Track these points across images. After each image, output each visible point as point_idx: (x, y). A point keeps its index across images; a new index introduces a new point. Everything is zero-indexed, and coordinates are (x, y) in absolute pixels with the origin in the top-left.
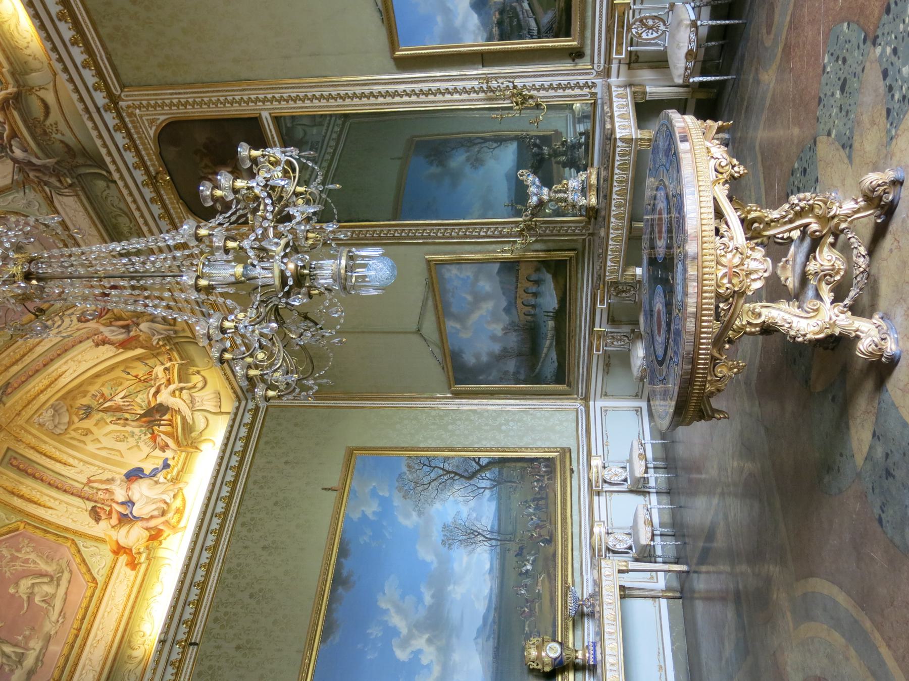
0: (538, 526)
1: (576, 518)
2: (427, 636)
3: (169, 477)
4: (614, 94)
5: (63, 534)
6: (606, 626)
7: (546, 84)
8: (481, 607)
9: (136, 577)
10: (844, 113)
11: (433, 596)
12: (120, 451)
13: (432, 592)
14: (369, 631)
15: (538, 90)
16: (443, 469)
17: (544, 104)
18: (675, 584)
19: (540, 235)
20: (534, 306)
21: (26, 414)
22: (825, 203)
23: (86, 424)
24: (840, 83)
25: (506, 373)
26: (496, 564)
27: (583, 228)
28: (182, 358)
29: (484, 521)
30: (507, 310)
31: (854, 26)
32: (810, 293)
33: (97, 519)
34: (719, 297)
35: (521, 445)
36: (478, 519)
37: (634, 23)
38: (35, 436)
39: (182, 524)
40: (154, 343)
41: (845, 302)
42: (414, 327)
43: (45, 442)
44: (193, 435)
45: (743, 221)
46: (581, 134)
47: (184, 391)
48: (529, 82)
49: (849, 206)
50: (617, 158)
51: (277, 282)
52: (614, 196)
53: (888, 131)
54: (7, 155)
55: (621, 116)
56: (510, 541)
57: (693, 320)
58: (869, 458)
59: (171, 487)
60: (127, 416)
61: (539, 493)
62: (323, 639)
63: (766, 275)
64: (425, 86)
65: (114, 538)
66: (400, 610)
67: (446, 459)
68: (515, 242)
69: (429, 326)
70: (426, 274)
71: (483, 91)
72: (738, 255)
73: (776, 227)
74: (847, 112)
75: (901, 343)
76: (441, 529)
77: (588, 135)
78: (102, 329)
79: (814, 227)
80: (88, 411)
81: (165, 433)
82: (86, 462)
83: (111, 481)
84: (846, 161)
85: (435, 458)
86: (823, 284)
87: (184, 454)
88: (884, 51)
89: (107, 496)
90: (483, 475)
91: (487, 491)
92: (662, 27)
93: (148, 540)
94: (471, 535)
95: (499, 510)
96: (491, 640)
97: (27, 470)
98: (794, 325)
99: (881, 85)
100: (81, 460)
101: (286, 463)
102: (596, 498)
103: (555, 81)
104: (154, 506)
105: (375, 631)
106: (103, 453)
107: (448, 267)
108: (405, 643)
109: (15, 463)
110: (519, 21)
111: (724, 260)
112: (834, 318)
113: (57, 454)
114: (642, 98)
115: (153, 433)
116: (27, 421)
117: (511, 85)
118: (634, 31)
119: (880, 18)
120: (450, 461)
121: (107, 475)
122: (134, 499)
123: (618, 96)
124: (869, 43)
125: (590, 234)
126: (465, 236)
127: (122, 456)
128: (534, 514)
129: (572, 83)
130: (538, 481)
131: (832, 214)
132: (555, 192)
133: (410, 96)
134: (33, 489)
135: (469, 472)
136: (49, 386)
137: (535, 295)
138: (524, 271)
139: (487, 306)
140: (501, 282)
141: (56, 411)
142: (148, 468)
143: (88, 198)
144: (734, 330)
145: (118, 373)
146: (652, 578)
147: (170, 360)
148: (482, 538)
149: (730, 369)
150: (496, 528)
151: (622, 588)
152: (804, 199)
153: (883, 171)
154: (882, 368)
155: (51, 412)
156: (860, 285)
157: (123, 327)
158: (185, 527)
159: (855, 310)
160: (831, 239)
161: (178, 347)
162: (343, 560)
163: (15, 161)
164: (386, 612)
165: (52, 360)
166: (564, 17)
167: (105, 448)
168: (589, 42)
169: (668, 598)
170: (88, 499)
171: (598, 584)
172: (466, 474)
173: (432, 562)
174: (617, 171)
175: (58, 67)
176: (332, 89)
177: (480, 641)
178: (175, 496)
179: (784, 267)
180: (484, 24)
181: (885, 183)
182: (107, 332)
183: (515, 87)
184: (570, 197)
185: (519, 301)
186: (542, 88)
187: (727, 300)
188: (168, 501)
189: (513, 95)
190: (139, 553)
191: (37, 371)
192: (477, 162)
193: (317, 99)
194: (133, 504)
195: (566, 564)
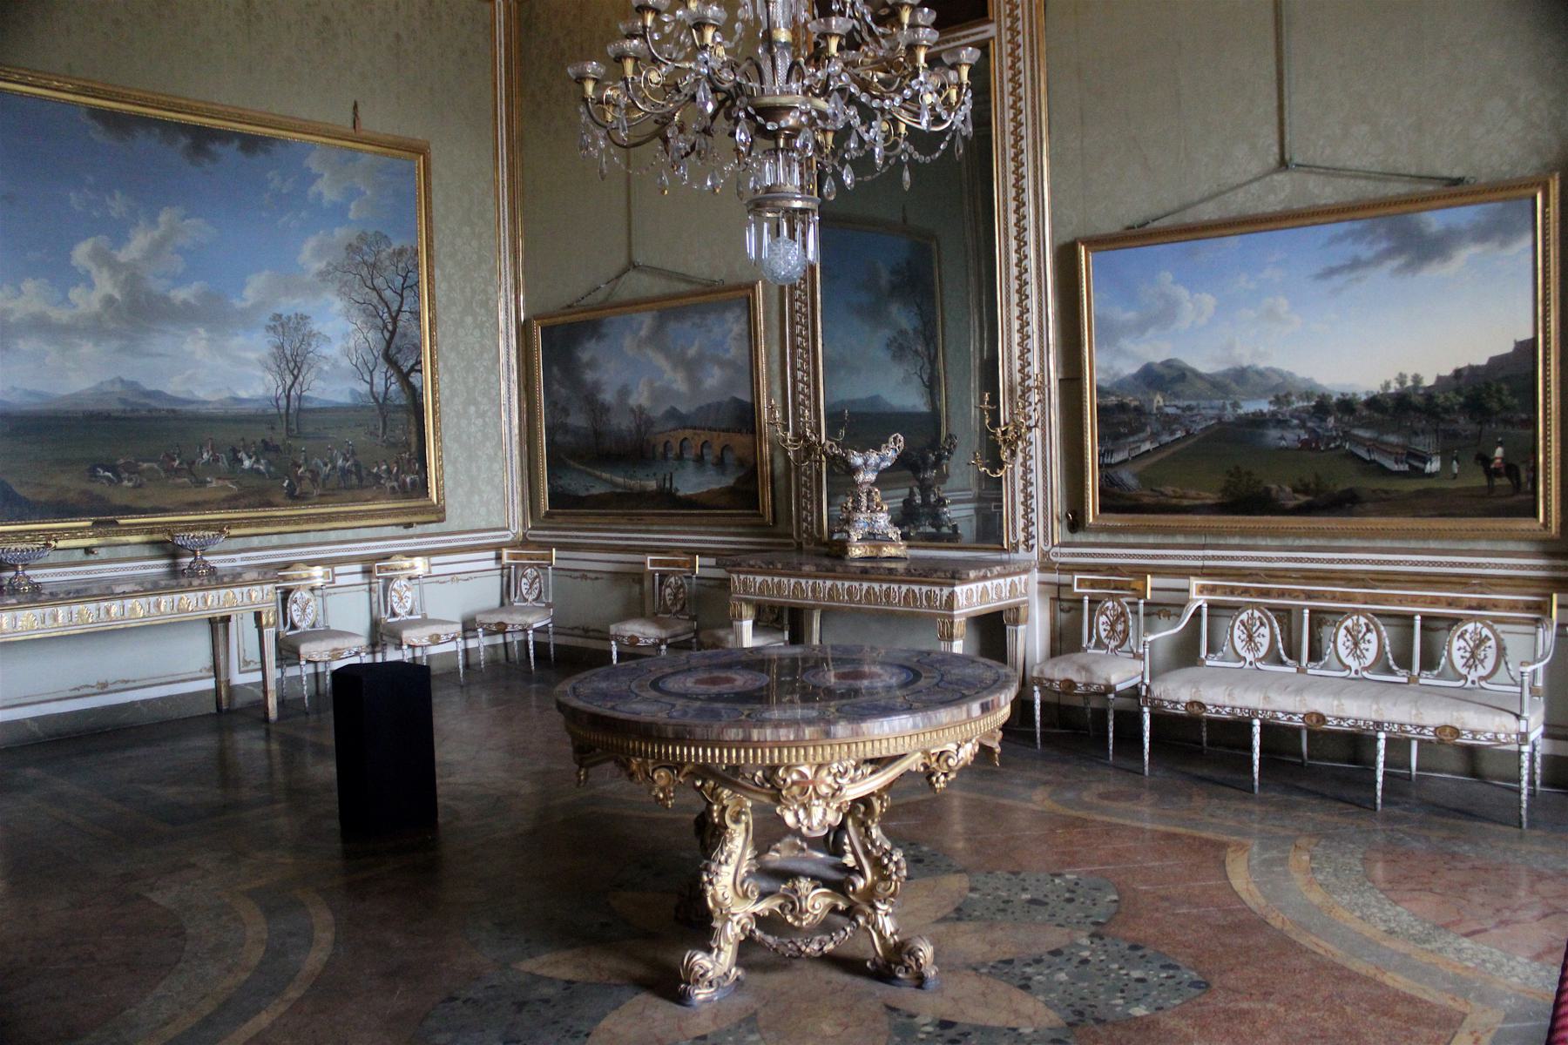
0: (315, 474)
1: (333, 536)
2: (118, 296)
4: (1016, 579)
6: (168, 598)
7: (1032, 477)
8: (174, 386)
10: (1002, 906)
11: (185, 303)
13: (193, 301)
14: (118, 194)
15: (1024, 464)
16: (399, 310)
17: (1001, 473)
18: (239, 701)
19: (797, 468)
20: (680, 457)
22: (892, 895)
24: (1041, 897)
25: (565, 411)
26: (250, 408)
27: (811, 534)
30: (673, 414)
31: (1113, 907)
32: (765, 885)
34: (774, 769)
35: (446, 440)
36: (320, 374)
37: (1120, 604)
41: (758, 933)
42: (639, 259)
45: (872, 794)
46: (955, 527)
48: (1036, 450)
49: (888, 925)
50: (925, 589)
51: (767, 100)
52: (865, 585)
53: (984, 964)
55: (985, 591)
56: (288, 429)
57: (740, 737)
58: (538, 979)
61: (370, 473)
62: (95, 113)
63: (804, 830)
64: (1032, 289)
66: (156, 249)
67: (417, 315)
68: (786, 428)
70: (730, 281)
71: (1023, 380)
72: (830, 791)
73: (858, 833)
74: (1004, 910)
75: (706, 1006)
76: (300, 310)
77: (952, 538)
79: (860, 884)
84: (939, 915)
85: (418, 296)
86: (780, 901)
88: (1085, 948)
90: (393, 379)
92: (1113, 644)
94: (293, 363)
95: (338, 409)
96: (121, 407)
98: (724, 868)
99: (1040, 950)
101: (398, 36)
102: (358, 567)
103: (1037, 490)
105: (118, 205)
107: (744, 318)
108: (103, 258)
110: (1126, 435)
111: (824, 773)
112: (735, 919)
114: (1009, 620)
117: (1032, 423)
118: (1110, 604)
119: (1125, 939)
120: (414, 323)
123: (1013, 583)
124: (1093, 929)
125: (800, 544)
126: (794, 347)
128: (334, 467)
129: (1034, 515)
130: (389, 471)
131: (879, 905)
132: (869, 493)
133: (1019, 264)
135: (398, 355)
137: (700, 460)
138: (740, 441)
139: (679, 382)
140: (720, 404)
144: (714, 789)
146: (247, 663)
148: (289, 382)
149: (663, 789)
150: (307, 405)
151: (227, 619)
152: (898, 868)
153: (935, 963)
154: (671, 985)
156: (782, 949)
159: (746, 946)
160: (842, 906)
162: (236, 143)
164: (153, 222)
166: (1128, 503)
168: (1092, 539)
169: (217, 690)
171: (234, 579)
172: (393, 351)
173: (244, 300)
174: (904, 588)
176: (1030, 140)
177: (118, 388)
179: (794, 846)
180: (1121, 385)
181: (919, 966)
183: (1029, 428)
184: (862, 517)
185: (688, 433)
186: (1027, 470)
187: (768, 781)
189: (1017, 427)
192: (898, 349)
193: (1016, 116)
195: (258, 525)
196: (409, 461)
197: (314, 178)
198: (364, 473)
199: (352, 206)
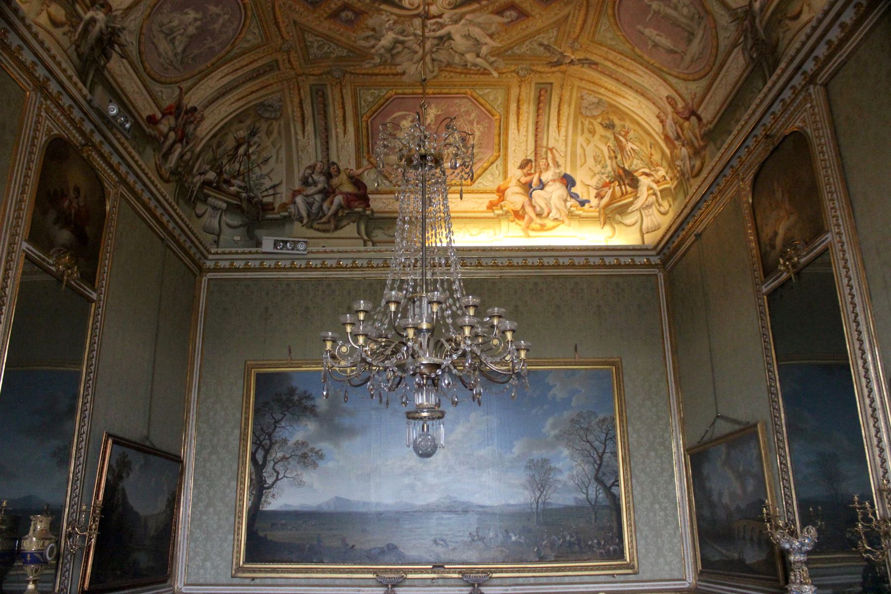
3: (572, 209)
5: (502, 147)
9: (483, 212)
12: (585, 162)
16: (604, 452)
21: (583, 84)
23: (600, 130)
28: (675, 188)
29: (555, 495)
33: (522, 167)
38: (571, 97)
39: (531, 233)
40: (677, 163)
43: (570, 105)
44: (618, 217)
47: (654, 197)
59: (563, 214)
60: (619, 157)
65: (510, 185)
67: (615, 454)
69: (724, 428)
76: (544, 456)
78: (670, 117)
80: (610, 126)
81: (613, 193)
82: (566, 141)
83: (557, 165)
85: (616, 443)
87: (597, 214)
89: (543, 167)
91: (585, 496)
93: (514, 211)
97: (541, 102)
100: (566, 136)
104: (544, 206)
106: (579, 151)
109: (543, 92)
113: (564, 118)
115: (611, 182)
116: (579, 87)
121: (561, 161)
122: (547, 188)
127: (581, 166)
128: (564, 541)
130: (599, 543)
134: (528, 113)
136: (613, 92)
141: (598, 103)
142: (577, 189)
143: (747, 77)
145: (648, 141)
147: (671, 179)
148: (538, 495)
155: (595, 100)
157: (678, 134)
158: (529, 236)
161: (680, 184)
165: (631, 87)
167: (584, 151)
170: (536, 154)
172: (600, 475)
175: (814, 23)
178: (556, 219)
182: (669, 122)
188: (551, 215)
190: (501, 208)
191: (617, 80)
194: (542, 189)
196: (612, 537)
197: (550, 388)
198: (583, 545)
199: (574, 399)
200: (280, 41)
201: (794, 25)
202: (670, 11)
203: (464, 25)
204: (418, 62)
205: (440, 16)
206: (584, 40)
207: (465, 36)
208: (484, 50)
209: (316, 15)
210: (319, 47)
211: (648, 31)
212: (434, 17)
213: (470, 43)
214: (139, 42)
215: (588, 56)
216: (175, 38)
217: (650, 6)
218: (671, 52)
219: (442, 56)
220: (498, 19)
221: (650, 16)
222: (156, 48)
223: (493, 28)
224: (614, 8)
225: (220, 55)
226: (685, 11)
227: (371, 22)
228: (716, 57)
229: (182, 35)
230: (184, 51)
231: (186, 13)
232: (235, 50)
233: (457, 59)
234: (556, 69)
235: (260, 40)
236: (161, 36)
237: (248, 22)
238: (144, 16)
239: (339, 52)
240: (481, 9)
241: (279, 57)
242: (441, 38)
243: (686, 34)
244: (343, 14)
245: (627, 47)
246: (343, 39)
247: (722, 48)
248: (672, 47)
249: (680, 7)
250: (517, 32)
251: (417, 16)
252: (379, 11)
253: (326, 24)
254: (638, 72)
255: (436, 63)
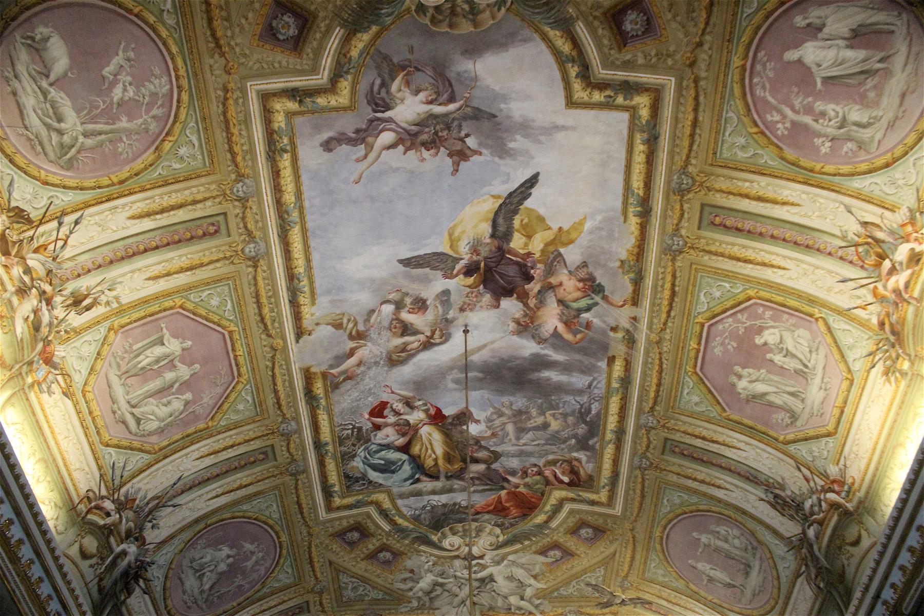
54: (803, 525)
163: (804, 533)
175: (879, 547)
200: (313, 581)
201: (857, 551)
202: (721, 544)
203: (506, 566)
204: (459, 606)
205: (481, 557)
206: (633, 578)
207: (508, 577)
208: (529, 592)
209: (353, 556)
210: (355, 589)
211: (700, 566)
212: (476, 558)
213: (513, 585)
214: (166, 577)
215: (640, 595)
216: (204, 574)
217: (699, 539)
218: (730, 586)
219: (484, 599)
220: (542, 559)
221: (700, 550)
222: (183, 583)
223: (537, 569)
224: (661, 544)
225: (249, 594)
226: (736, 542)
227: (409, 563)
228: (779, 589)
229: (211, 571)
230: (212, 587)
231: (220, 550)
232: (265, 590)
233: (500, 603)
234: (607, 610)
235: (292, 579)
236: (190, 572)
237: (282, 560)
238: (176, 551)
239: (374, 594)
240: (523, 549)
241: (310, 597)
242: (482, 580)
243: (742, 567)
244: (381, 555)
245: (680, 584)
246: (379, 581)
247: (783, 579)
248: (728, 581)
249: (730, 538)
250: (562, 573)
251: (457, 557)
252: (418, 552)
253: (363, 564)
254: (697, 610)
255: (477, 606)
